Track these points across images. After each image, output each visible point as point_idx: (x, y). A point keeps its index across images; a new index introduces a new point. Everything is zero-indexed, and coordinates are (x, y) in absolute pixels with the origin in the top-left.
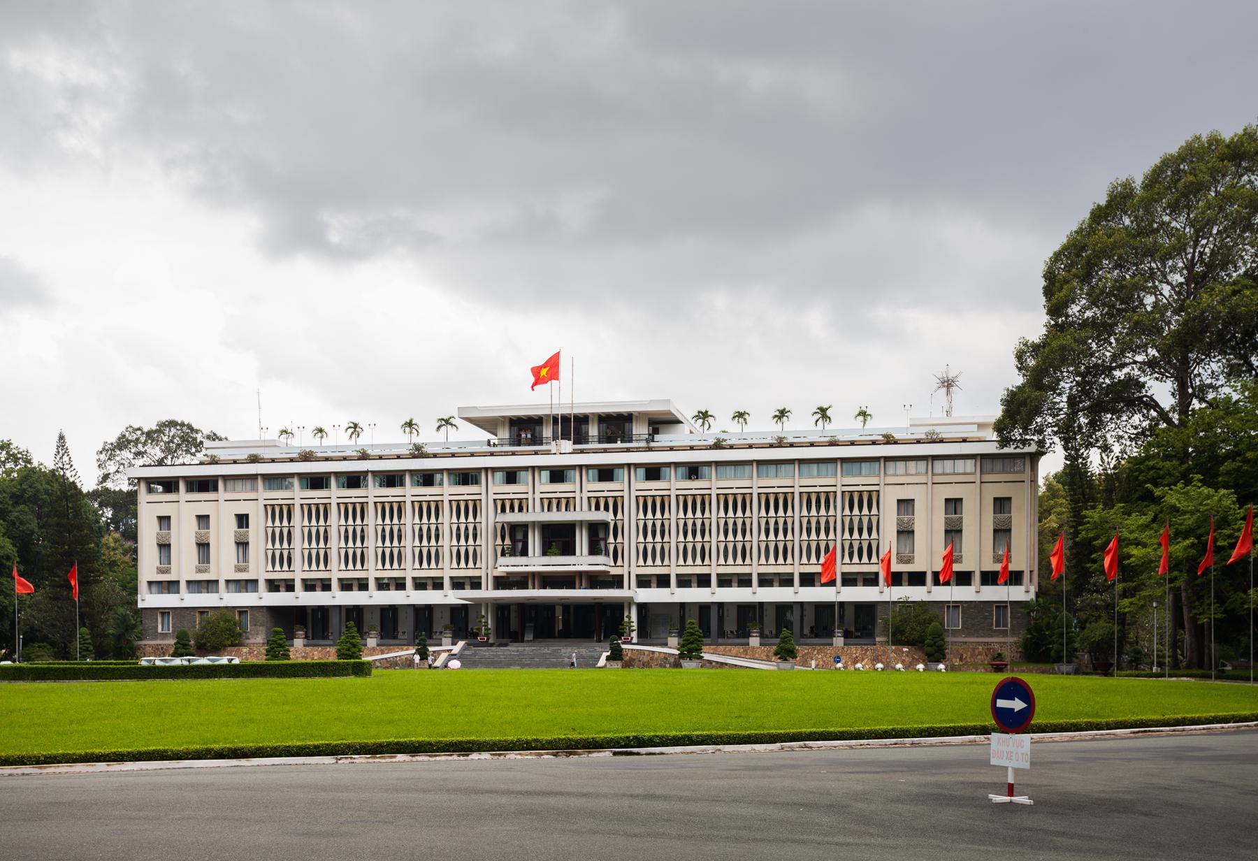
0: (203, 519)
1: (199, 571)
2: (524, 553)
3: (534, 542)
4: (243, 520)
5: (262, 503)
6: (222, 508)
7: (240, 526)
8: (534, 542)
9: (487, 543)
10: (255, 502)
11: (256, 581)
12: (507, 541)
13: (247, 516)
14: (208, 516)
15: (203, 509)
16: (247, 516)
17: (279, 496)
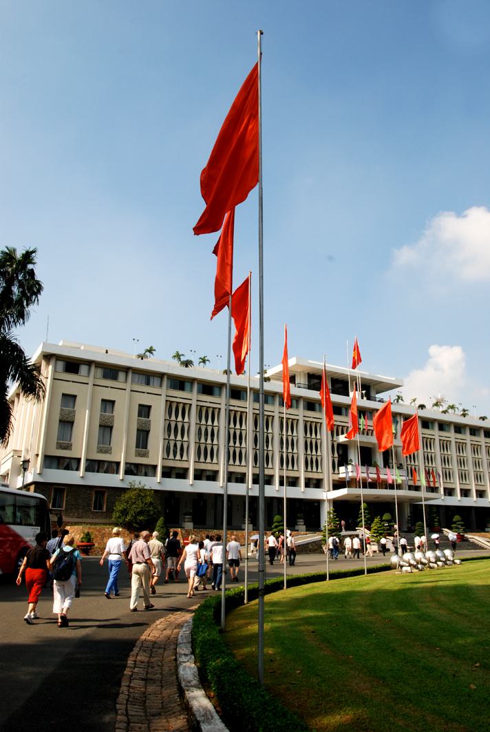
0: (108, 404)
1: (100, 451)
2: (343, 460)
3: (354, 456)
4: (145, 410)
5: (163, 398)
6: (126, 399)
7: (140, 415)
8: (354, 456)
9: (326, 455)
10: (158, 399)
11: (155, 467)
12: (336, 455)
13: (149, 407)
14: (113, 402)
15: (109, 394)
16: (149, 407)
17: (179, 395)
